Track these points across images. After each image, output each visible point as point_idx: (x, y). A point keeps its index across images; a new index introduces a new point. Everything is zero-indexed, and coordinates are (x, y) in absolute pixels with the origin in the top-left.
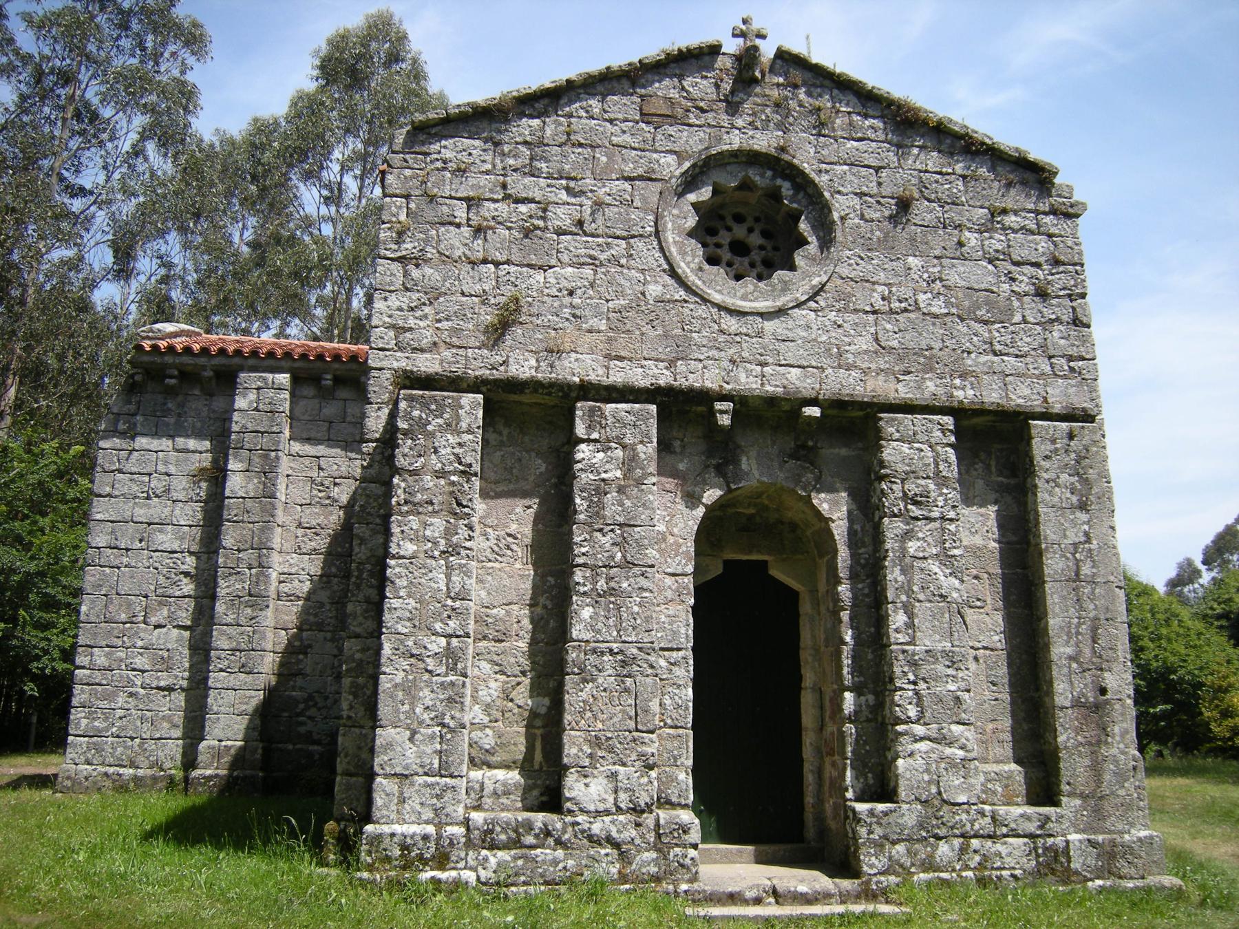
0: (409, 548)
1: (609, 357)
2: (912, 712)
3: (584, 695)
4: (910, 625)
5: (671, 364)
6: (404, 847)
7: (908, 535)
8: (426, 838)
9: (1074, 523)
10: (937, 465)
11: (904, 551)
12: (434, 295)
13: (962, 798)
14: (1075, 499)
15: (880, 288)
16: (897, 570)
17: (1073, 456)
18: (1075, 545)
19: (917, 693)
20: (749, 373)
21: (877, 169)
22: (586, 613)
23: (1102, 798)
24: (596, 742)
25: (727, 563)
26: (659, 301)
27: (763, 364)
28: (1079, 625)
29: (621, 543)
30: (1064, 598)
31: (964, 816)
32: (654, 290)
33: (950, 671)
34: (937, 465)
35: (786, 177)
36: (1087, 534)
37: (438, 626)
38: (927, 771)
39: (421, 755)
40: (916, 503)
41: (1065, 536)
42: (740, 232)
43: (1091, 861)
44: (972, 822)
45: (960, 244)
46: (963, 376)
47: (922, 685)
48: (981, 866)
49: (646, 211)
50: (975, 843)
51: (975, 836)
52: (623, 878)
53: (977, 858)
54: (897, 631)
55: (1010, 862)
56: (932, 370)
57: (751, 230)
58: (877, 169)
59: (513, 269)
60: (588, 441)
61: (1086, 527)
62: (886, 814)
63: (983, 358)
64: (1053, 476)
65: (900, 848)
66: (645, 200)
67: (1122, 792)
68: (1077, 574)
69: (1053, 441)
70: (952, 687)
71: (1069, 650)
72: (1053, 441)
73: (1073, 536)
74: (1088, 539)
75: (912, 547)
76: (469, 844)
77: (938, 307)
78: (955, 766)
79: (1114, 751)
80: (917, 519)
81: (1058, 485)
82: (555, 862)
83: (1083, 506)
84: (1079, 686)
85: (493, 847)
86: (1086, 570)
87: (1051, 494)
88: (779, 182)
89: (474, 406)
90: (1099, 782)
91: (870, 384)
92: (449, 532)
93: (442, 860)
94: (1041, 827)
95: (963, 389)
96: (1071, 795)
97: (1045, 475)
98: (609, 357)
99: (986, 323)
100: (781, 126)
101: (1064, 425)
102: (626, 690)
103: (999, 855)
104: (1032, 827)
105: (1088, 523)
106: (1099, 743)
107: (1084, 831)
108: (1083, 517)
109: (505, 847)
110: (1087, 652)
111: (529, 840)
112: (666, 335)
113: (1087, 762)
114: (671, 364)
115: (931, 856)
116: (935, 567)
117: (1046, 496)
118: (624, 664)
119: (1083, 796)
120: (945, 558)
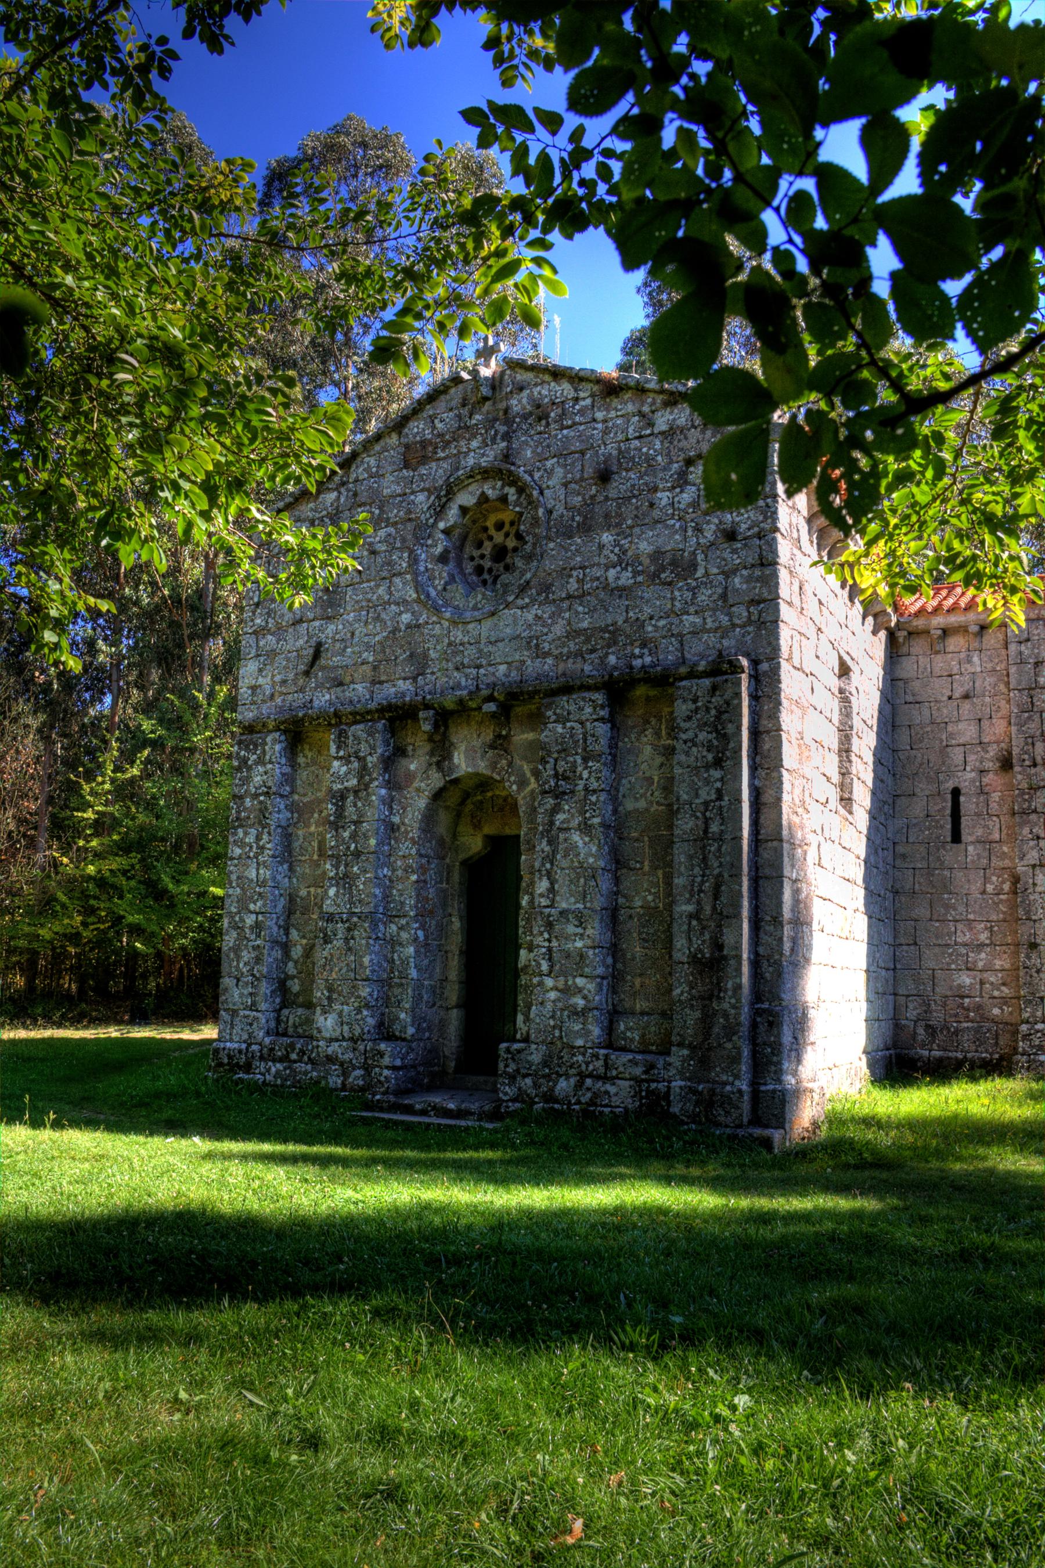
0: (238, 851)
1: (373, 683)
2: (545, 966)
3: (325, 953)
4: (552, 890)
5: (415, 679)
6: (230, 1057)
7: (556, 810)
8: (240, 1051)
9: (707, 782)
10: (585, 740)
11: (552, 823)
12: (272, 654)
13: (580, 1042)
14: (710, 757)
15: (575, 573)
16: (544, 842)
17: (713, 712)
18: (706, 804)
19: (550, 949)
20: (467, 676)
21: (583, 453)
22: (332, 892)
23: (709, 1049)
24: (330, 990)
25: (489, 839)
26: (409, 626)
27: (478, 667)
28: (703, 882)
29: (354, 836)
30: (691, 857)
31: (580, 1058)
32: (406, 618)
33: (580, 930)
34: (585, 740)
35: (510, 485)
36: (719, 791)
37: (252, 907)
38: (553, 1017)
39: (241, 995)
40: (566, 778)
41: (697, 796)
42: (499, 538)
43: (689, 1106)
44: (587, 1064)
45: (652, 505)
46: (643, 645)
47: (554, 943)
48: (592, 1102)
49: (401, 549)
50: (589, 1082)
51: (590, 1076)
52: (344, 1088)
53: (589, 1095)
54: (541, 895)
55: (616, 1101)
56: (615, 643)
57: (507, 535)
58: (583, 453)
59: (317, 623)
60: (337, 758)
61: (718, 785)
62: (519, 1051)
63: (662, 623)
64: (690, 735)
65: (528, 1081)
66: (404, 540)
67: (729, 1045)
68: (706, 831)
69: (695, 701)
70: (579, 944)
71: (690, 908)
72: (695, 701)
73: (705, 794)
74: (720, 798)
75: (561, 817)
76: (262, 1058)
77: (626, 578)
78: (576, 1013)
79: (726, 1006)
80: (564, 793)
81: (695, 745)
82: (306, 1073)
83: (718, 763)
84: (696, 943)
85: (274, 1061)
86: (714, 828)
87: (687, 754)
88: (507, 489)
89: (274, 741)
90: (707, 1035)
91: (561, 667)
92: (258, 838)
93: (248, 1068)
94: (646, 1072)
95: (641, 656)
96: (680, 1045)
97: (684, 736)
98: (373, 683)
99: (670, 584)
100: (507, 437)
101: (707, 682)
102: (350, 949)
103: (607, 1092)
104: (638, 1071)
105: (722, 779)
106: (710, 998)
107: (689, 1079)
108: (717, 774)
109: (281, 1060)
110: (708, 909)
111: (294, 1056)
112: (411, 655)
113: (698, 1014)
114: (415, 679)
115: (552, 1090)
116: (576, 837)
117: (683, 758)
118: (349, 929)
119: (690, 1046)
120: (585, 828)
